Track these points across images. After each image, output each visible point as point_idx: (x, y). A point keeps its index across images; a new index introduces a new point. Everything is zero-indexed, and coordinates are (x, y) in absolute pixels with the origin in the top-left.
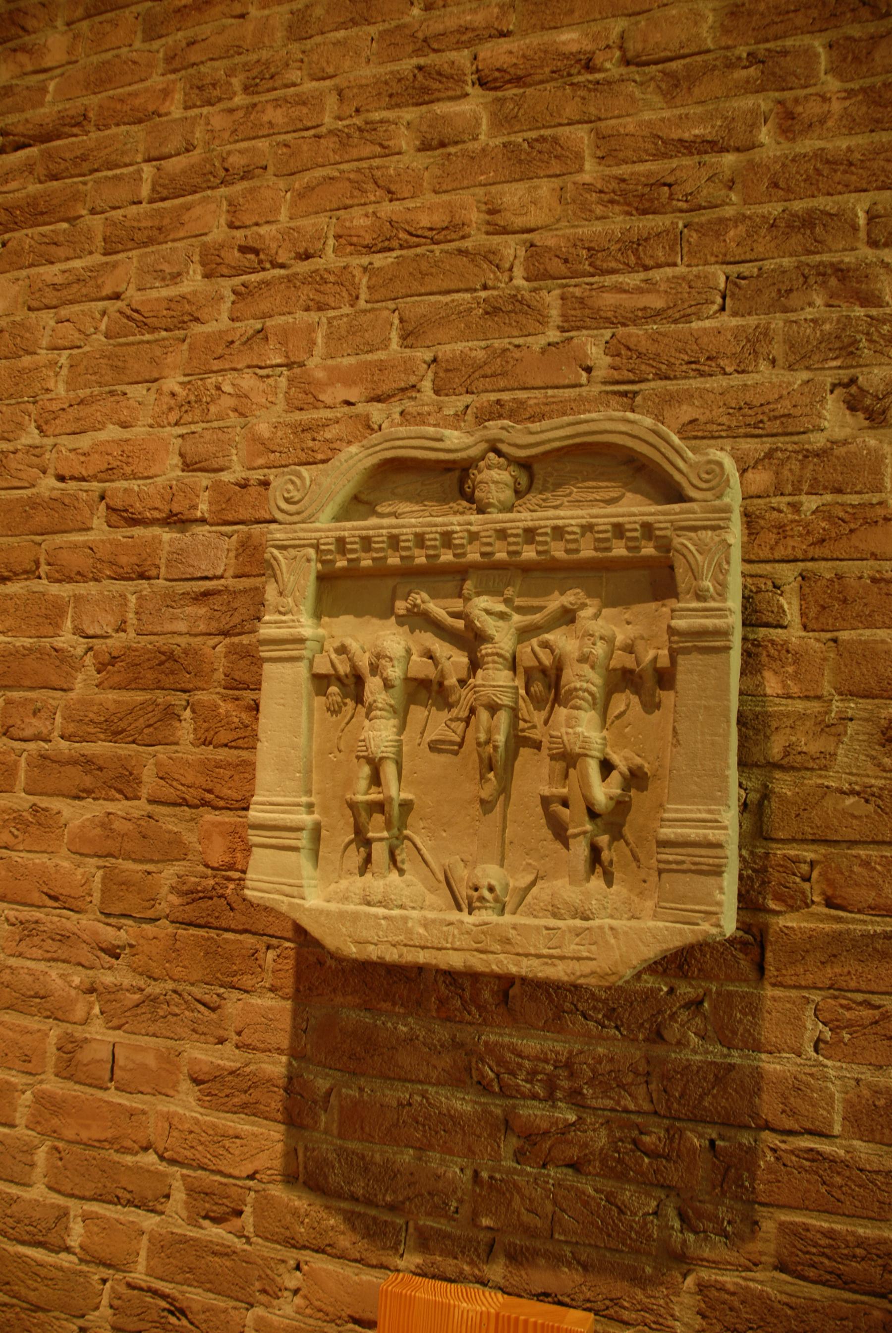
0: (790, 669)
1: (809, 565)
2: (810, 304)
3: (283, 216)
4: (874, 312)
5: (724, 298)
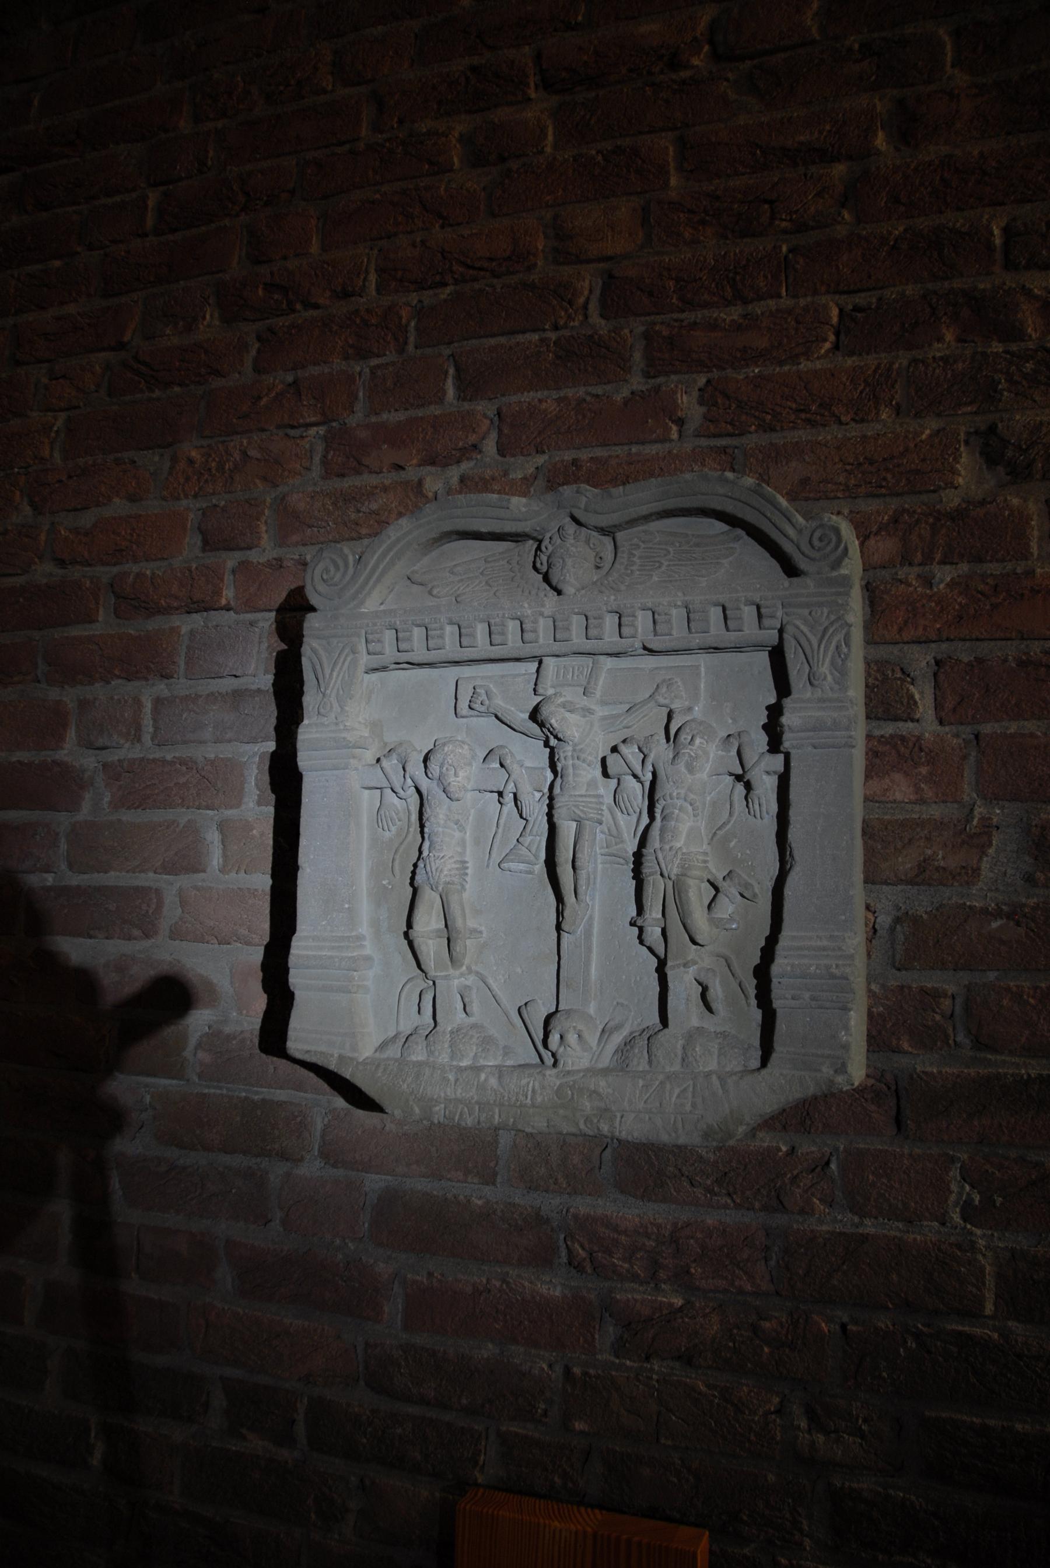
0: (924, 770)
1: (944, 646)
2: (940, 339)
3: (314, 248)
4: (1014, 347)
5: (837, 334)
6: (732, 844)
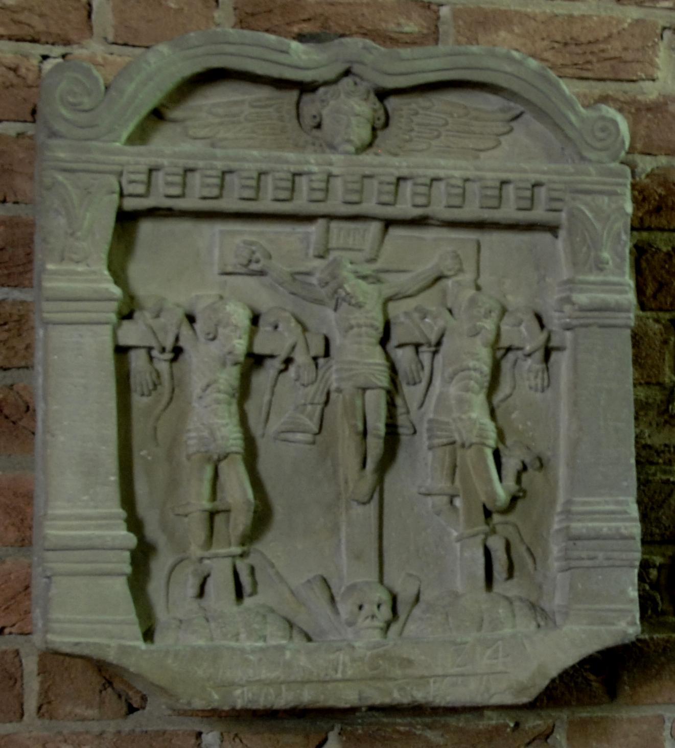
1: (645, 235)
6: (514, 416)
